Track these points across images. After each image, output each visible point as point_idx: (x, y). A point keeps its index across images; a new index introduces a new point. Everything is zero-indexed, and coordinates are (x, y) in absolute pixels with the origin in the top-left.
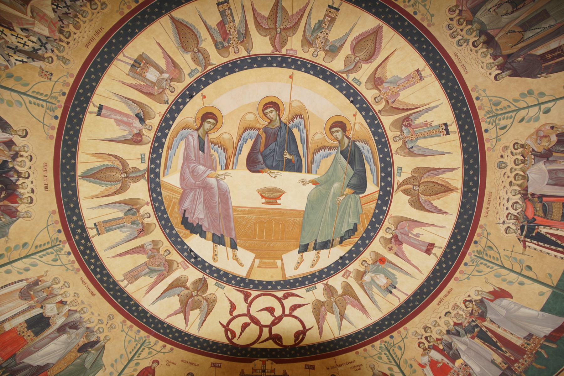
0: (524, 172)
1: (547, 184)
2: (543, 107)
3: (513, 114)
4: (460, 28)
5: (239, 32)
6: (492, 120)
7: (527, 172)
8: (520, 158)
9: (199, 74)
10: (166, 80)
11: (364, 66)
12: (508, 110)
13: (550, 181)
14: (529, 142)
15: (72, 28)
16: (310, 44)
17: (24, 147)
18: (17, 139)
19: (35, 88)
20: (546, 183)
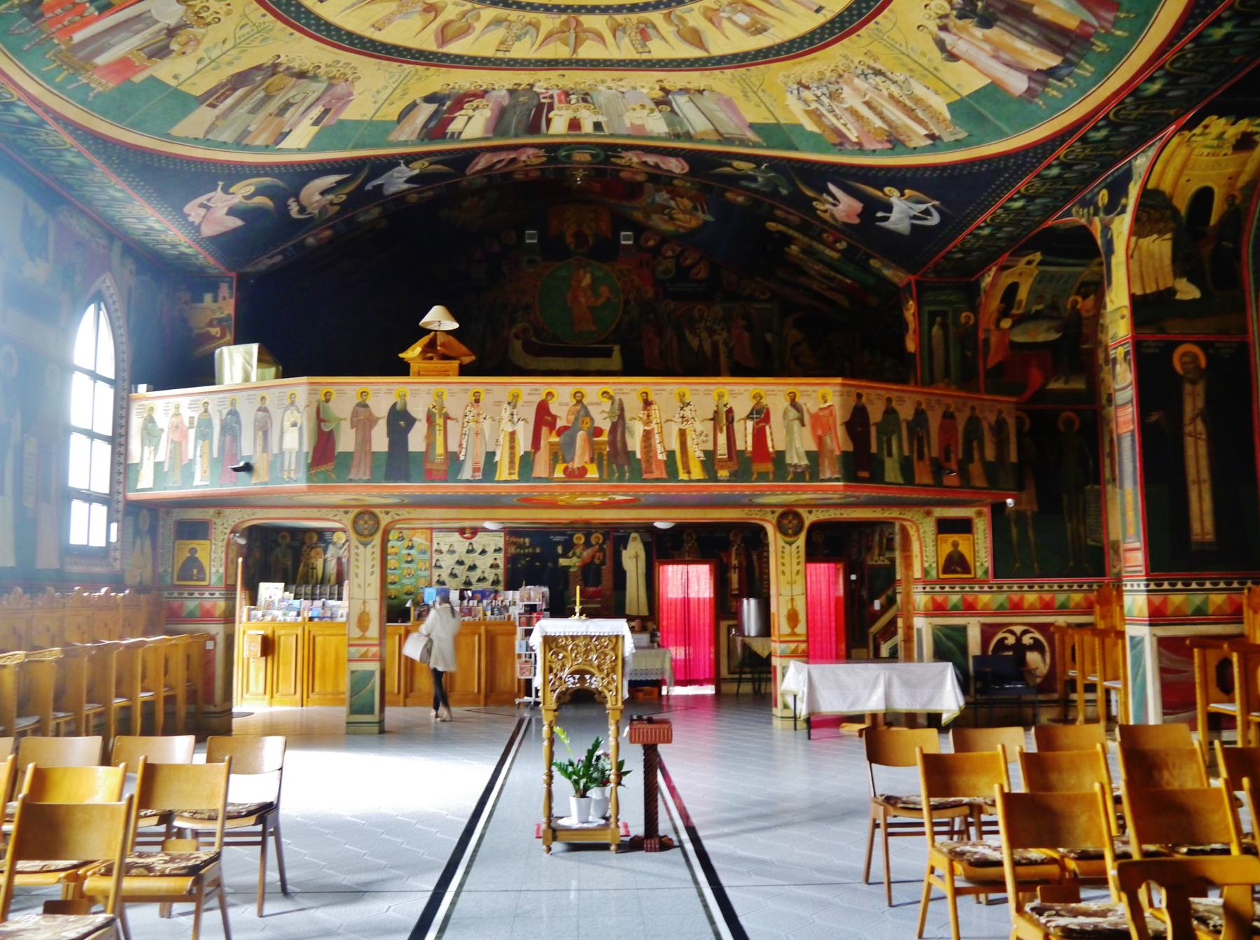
0: (189, 6)
1: (150, 11)
2: (208, 61)
3: (238, 41)
4: (342, 70)
5: (624, 32)
6: (263, 26)
7: (184, 7)
8: (204, 14)
9: (680, 8)
10: (724, 11)
11: (453, 17)
12: (248, 41)
13: (149, 15)
14: (202, 31)
15: (828, 74)
16: (530, 24)
17: (929, 18)
18: (935, 29)
19: (889, 52)
20: (153, 11)
